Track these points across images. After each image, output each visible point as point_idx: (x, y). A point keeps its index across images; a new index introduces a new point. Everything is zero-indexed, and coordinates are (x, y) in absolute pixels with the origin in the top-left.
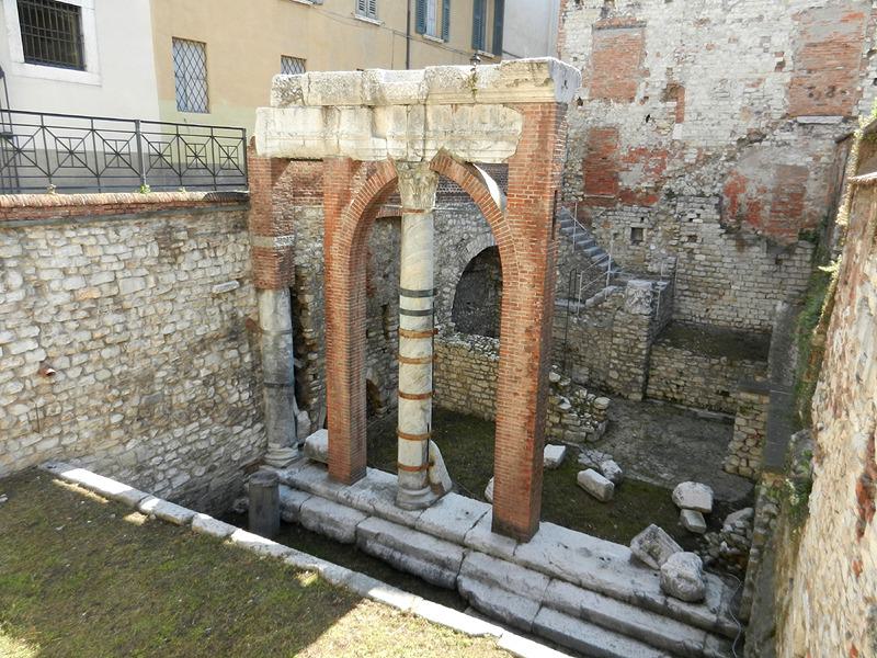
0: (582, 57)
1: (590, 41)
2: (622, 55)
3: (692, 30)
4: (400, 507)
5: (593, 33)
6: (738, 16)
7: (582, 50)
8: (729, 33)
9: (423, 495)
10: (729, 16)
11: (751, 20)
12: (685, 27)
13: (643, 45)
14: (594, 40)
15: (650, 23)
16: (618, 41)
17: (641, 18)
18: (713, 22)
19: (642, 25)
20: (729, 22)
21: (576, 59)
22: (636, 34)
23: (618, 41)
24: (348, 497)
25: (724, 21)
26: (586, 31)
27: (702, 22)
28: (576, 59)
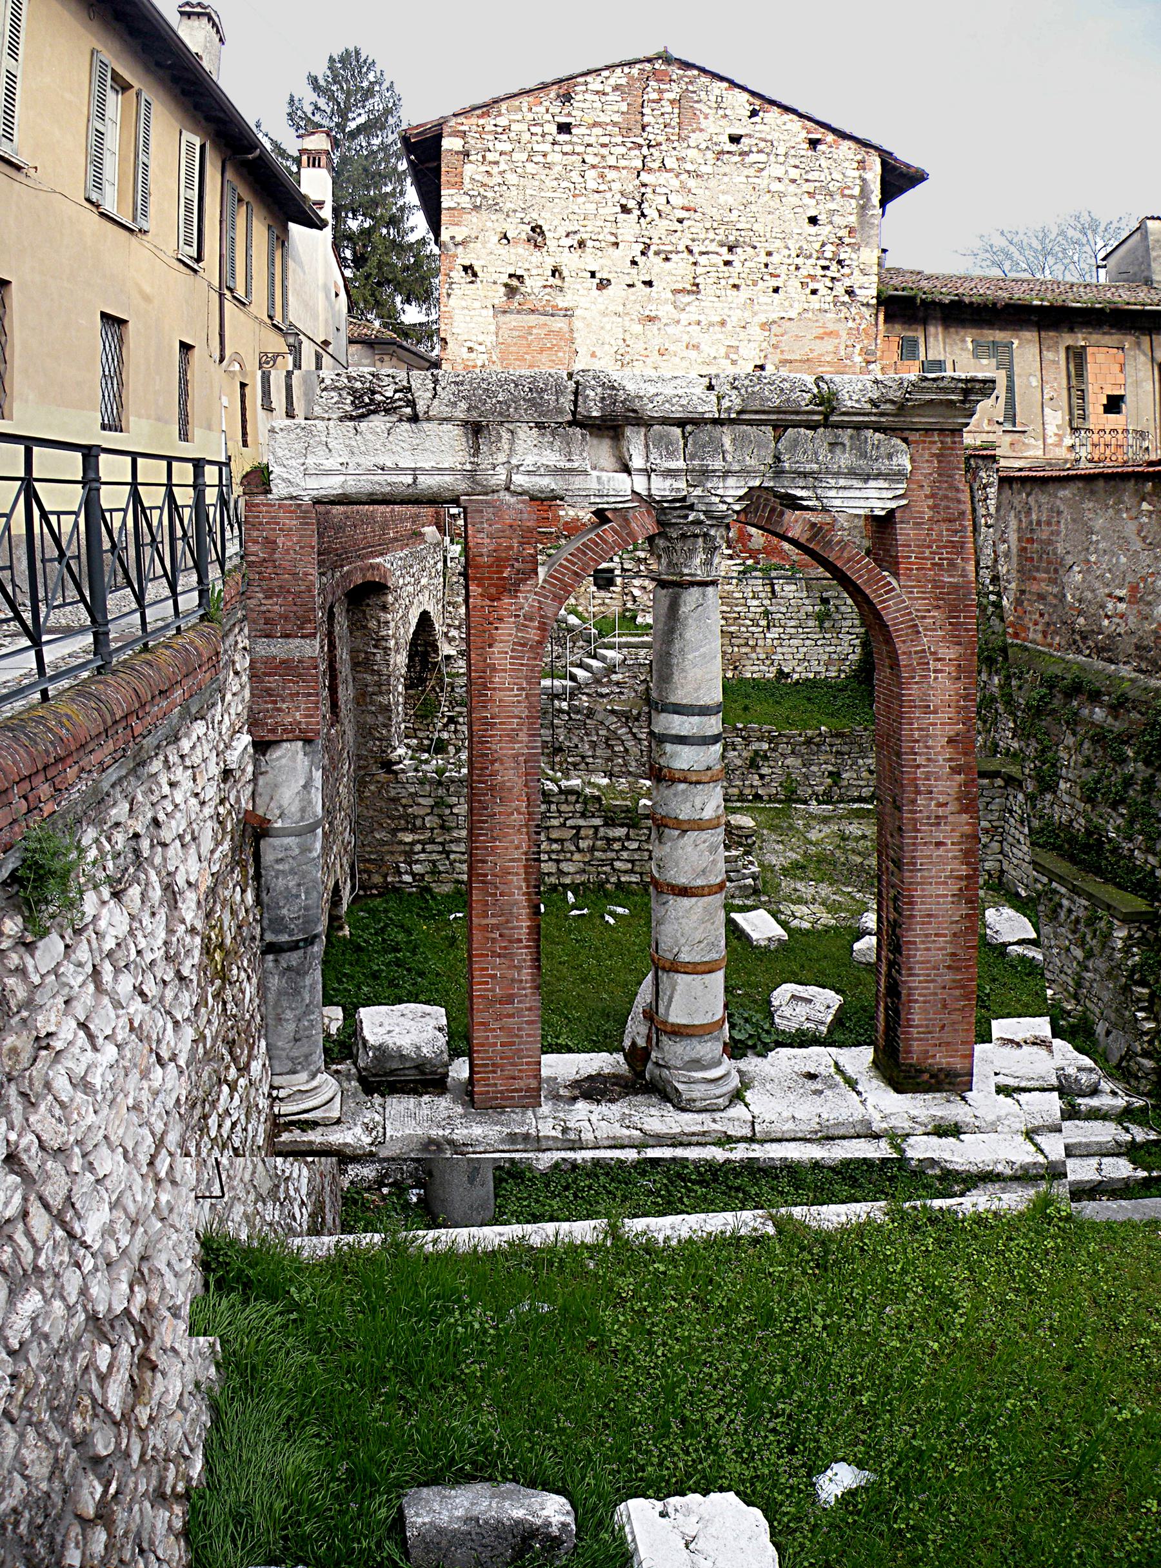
0: (482, 349)
1: (493, 328)
2: (542, 351)
3: (637, 328)
4: (704, 1110)
5: (495, 316)
6: (697, 318)
7: (481, 339)
8: (686, 338)
9: (727, 1075)
10: (684, 318)
11: (711, 324)
12: (627, 323)
13: (572, 341)
14: (498, 328)
15: (577, 313)
16: (535, 331)
17: (565, 305)
18: (664, 321)
19: (568, 313)
20: (684, 322)
21: (470, 349)
22: (559, 324)
23: (535, 331)
24: (565, 1130)
25: (678, 322)
26: (484, 312)
27: (651, 319)
28: (470, 349)
